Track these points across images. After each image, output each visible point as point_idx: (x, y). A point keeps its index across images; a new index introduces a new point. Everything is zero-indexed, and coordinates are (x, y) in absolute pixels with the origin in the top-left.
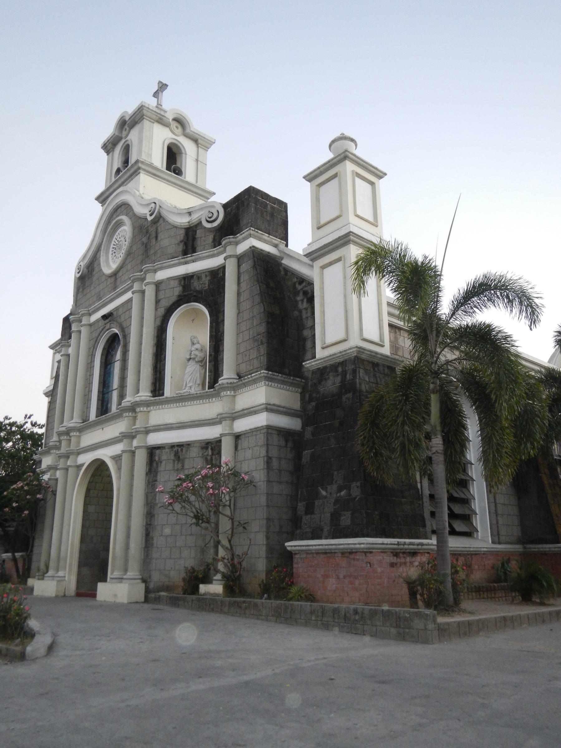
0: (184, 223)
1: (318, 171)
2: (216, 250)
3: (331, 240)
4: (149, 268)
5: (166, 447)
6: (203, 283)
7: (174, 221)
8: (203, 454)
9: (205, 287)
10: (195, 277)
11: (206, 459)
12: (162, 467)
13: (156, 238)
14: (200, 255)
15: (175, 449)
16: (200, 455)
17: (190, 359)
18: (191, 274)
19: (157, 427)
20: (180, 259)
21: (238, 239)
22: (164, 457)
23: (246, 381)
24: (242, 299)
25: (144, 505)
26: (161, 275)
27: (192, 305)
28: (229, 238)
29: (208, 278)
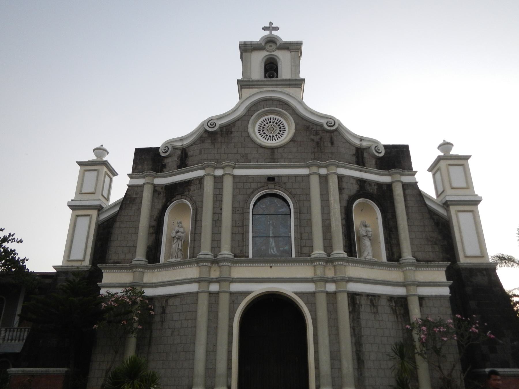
0: (358, 144)
1: (450, 157)
2: (383, 172)
3: (468, 199)
4: (335, 163)
5: (364, 295)
6: (372, 189)
7: (350, 139)
8: (389, 305)
9: (375, 192)
10: (367, 182)
11: (392, 308)
12: (362, 309)
13: (332, 143)
14: (372, 170)
15: (370, 297)
16: (388, 305)
17: (366, 236)
18: (365, 180)
19: (358, 280)
20: (355, 166)
21: (405, 173)
22: (363, 302)
23: (431, 264)
24: (410, 211)
25: (351, 336)
26: (342, 171)
27: (366, 200)
28: (401, 170)
29: (376, 187)
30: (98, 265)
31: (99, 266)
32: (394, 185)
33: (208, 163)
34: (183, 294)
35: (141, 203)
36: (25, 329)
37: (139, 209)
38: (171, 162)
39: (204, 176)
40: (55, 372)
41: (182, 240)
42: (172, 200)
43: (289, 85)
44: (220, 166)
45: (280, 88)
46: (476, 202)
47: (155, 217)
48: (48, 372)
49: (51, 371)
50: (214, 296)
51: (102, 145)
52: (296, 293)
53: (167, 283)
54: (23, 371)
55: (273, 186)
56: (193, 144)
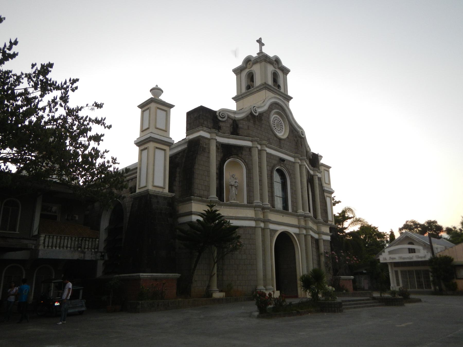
13: (301, 145)
30: (192, 197)
31: (193, 197)
32: (314, 177)
33: (258, 139)
34: (246, 227)
35: (209, 153)
36: (65, 237)
37: (209, 157)
38: (226, 127)
39: (252, 147)
40: (173, 277)
41: (237, 189)
42: (230, 157)
43: (285, 98)
44: (260, 143)
45: (283, 99)
46: (332, 192)
47: (217, 167)
48: (168, 277)
49: (170, 276)
50: (263, 230)
51: (157, 86)
52: (295, 234)
53: (234, 218)
54: (152, 276)
55: (282, 165)
56: (243, 119)
